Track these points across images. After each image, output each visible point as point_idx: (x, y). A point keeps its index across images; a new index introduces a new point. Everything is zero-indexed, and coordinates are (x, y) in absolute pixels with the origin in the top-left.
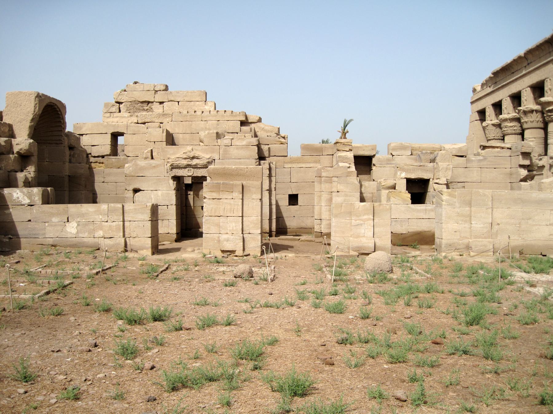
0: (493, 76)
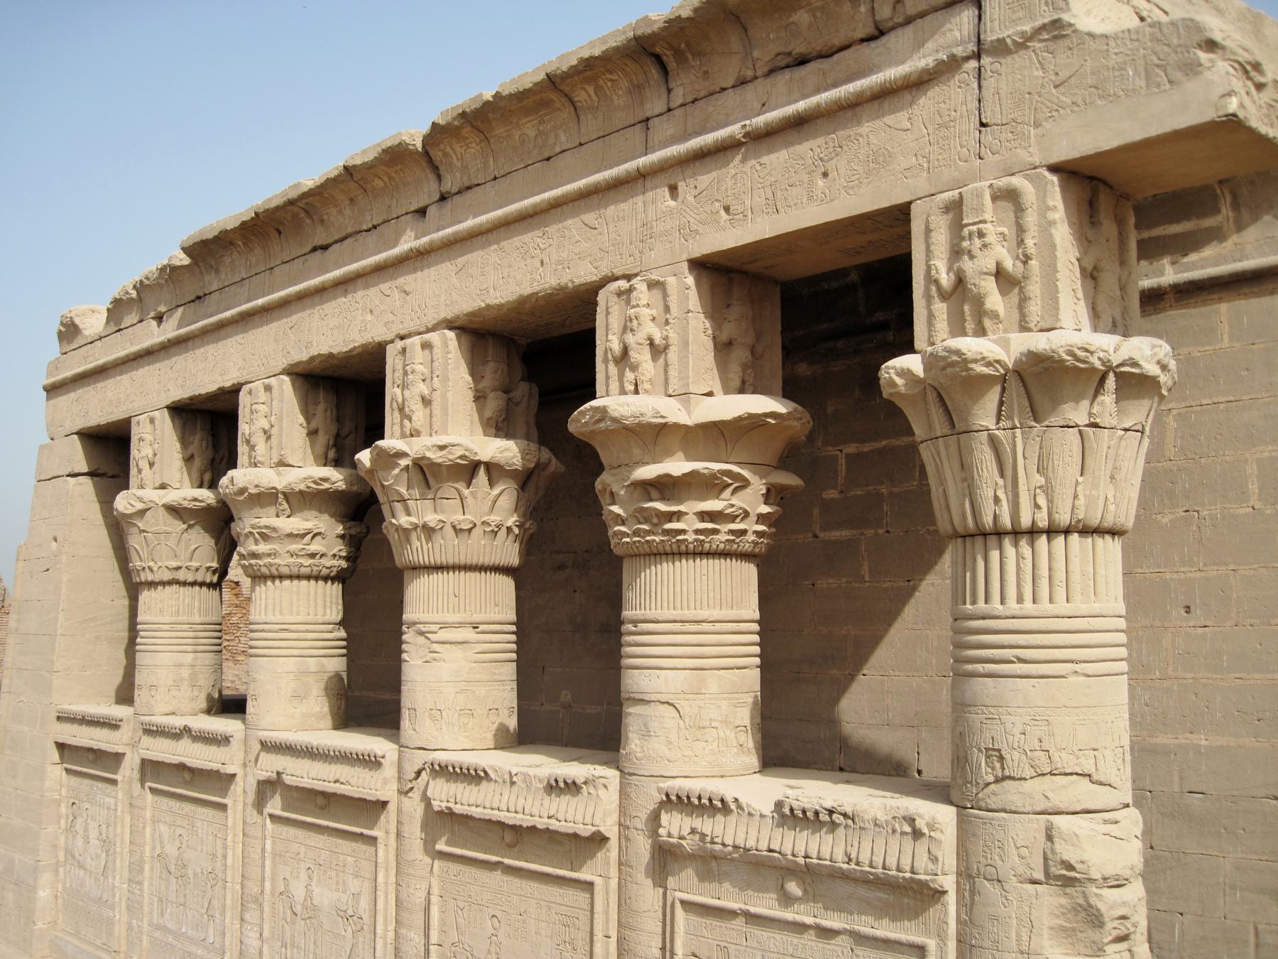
0: (184, 260)
